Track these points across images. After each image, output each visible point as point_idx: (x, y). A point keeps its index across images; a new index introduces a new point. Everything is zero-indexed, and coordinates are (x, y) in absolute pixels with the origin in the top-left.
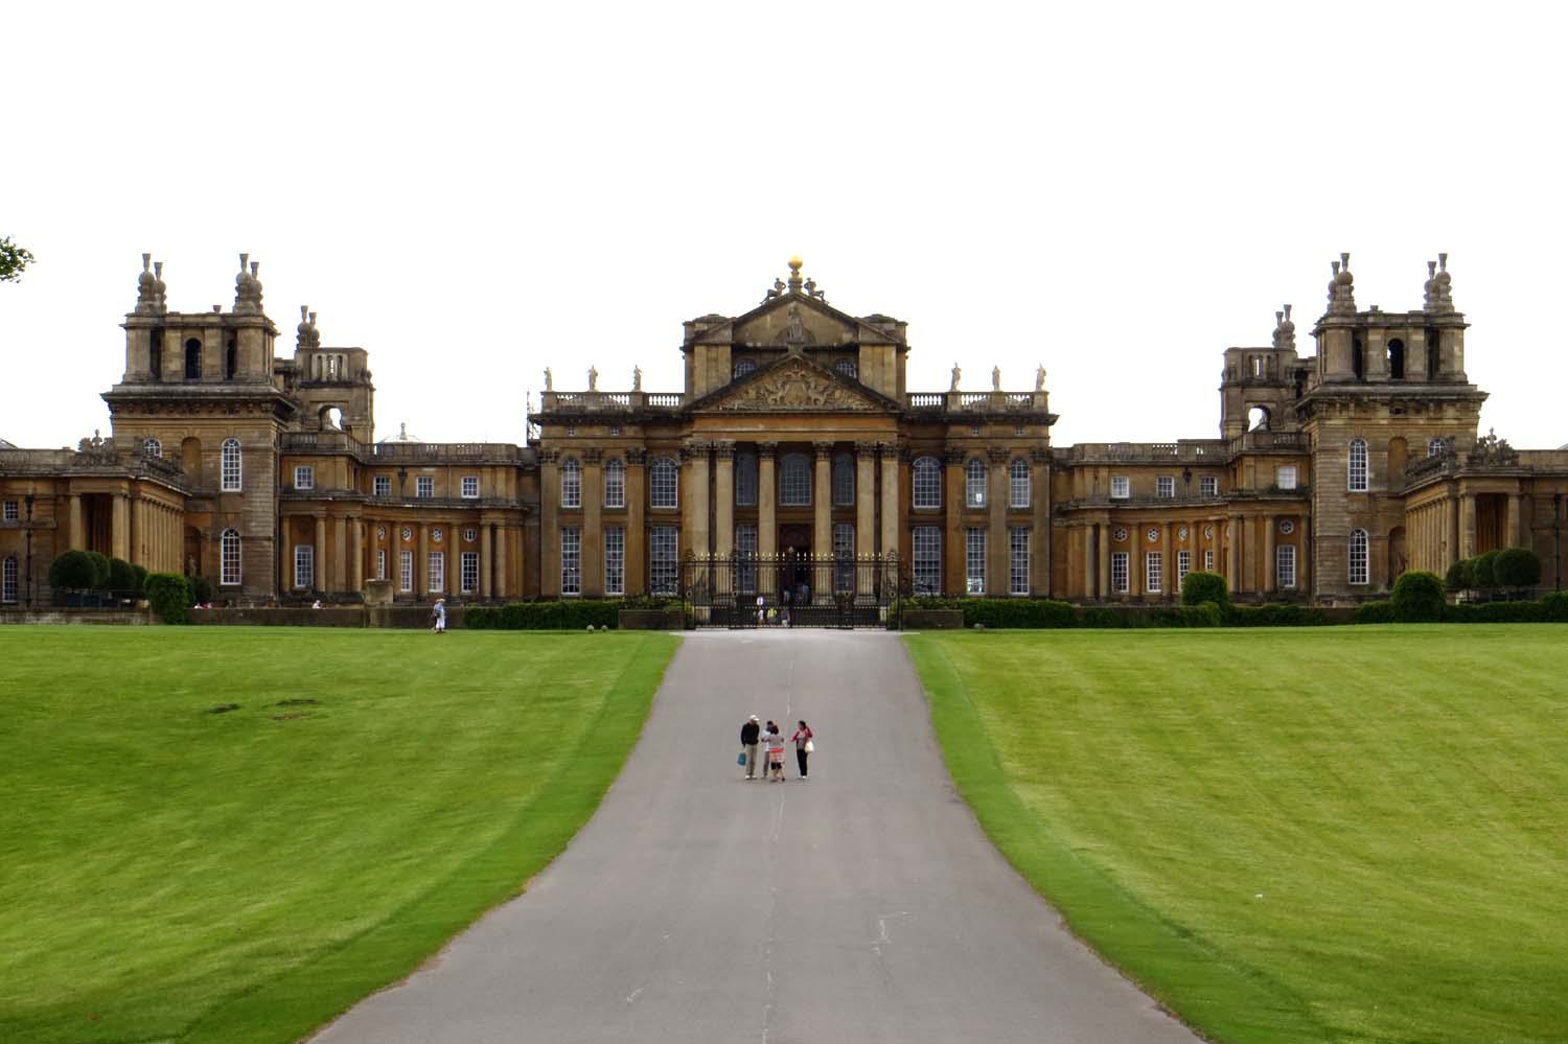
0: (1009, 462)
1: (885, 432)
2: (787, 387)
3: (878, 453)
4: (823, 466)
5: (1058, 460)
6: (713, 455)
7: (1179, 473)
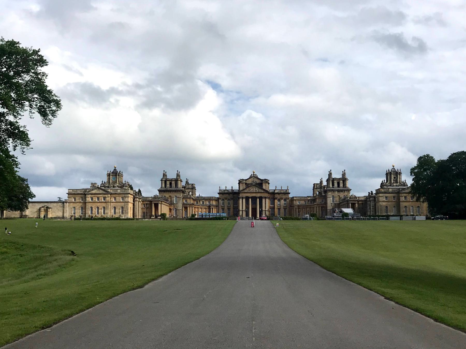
1: (266, 195)
3: (265, 198)
4: (258, 200)
6: (243, 198)
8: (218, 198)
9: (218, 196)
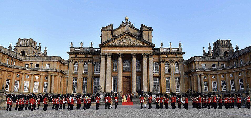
0: (174, 63)
2: (125, 40)
3: (148, 56)
4: (134, 60)
5: (185, 63)
6: (106, 57)
7: (217, 63)
8: (69, 61)
9: (66, 57)
